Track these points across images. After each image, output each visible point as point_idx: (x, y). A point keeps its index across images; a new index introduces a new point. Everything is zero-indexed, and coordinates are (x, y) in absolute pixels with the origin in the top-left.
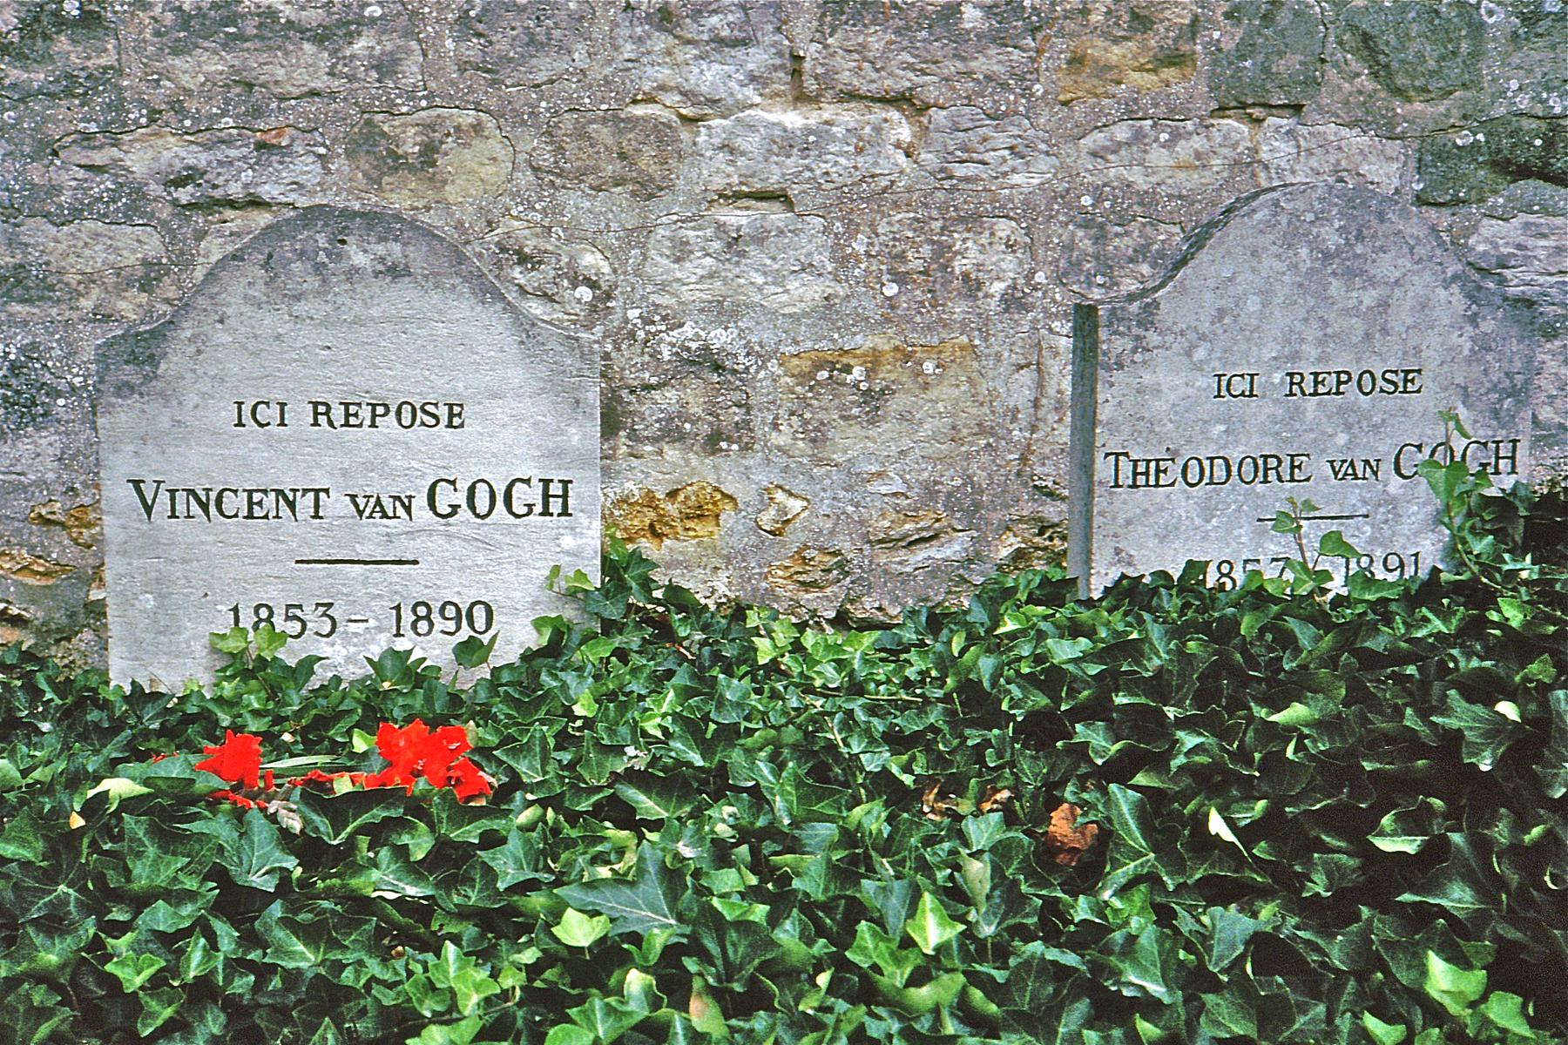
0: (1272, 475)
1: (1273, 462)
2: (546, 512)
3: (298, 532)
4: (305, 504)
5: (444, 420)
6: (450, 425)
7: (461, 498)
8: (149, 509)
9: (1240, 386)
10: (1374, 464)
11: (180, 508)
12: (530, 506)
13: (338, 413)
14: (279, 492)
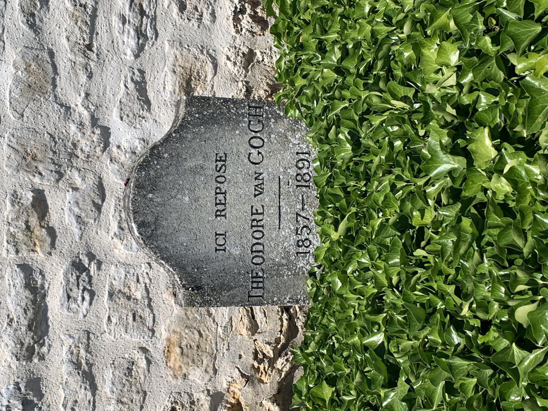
0: (259, 224)
1: (255, 223)
10: (257, 175)
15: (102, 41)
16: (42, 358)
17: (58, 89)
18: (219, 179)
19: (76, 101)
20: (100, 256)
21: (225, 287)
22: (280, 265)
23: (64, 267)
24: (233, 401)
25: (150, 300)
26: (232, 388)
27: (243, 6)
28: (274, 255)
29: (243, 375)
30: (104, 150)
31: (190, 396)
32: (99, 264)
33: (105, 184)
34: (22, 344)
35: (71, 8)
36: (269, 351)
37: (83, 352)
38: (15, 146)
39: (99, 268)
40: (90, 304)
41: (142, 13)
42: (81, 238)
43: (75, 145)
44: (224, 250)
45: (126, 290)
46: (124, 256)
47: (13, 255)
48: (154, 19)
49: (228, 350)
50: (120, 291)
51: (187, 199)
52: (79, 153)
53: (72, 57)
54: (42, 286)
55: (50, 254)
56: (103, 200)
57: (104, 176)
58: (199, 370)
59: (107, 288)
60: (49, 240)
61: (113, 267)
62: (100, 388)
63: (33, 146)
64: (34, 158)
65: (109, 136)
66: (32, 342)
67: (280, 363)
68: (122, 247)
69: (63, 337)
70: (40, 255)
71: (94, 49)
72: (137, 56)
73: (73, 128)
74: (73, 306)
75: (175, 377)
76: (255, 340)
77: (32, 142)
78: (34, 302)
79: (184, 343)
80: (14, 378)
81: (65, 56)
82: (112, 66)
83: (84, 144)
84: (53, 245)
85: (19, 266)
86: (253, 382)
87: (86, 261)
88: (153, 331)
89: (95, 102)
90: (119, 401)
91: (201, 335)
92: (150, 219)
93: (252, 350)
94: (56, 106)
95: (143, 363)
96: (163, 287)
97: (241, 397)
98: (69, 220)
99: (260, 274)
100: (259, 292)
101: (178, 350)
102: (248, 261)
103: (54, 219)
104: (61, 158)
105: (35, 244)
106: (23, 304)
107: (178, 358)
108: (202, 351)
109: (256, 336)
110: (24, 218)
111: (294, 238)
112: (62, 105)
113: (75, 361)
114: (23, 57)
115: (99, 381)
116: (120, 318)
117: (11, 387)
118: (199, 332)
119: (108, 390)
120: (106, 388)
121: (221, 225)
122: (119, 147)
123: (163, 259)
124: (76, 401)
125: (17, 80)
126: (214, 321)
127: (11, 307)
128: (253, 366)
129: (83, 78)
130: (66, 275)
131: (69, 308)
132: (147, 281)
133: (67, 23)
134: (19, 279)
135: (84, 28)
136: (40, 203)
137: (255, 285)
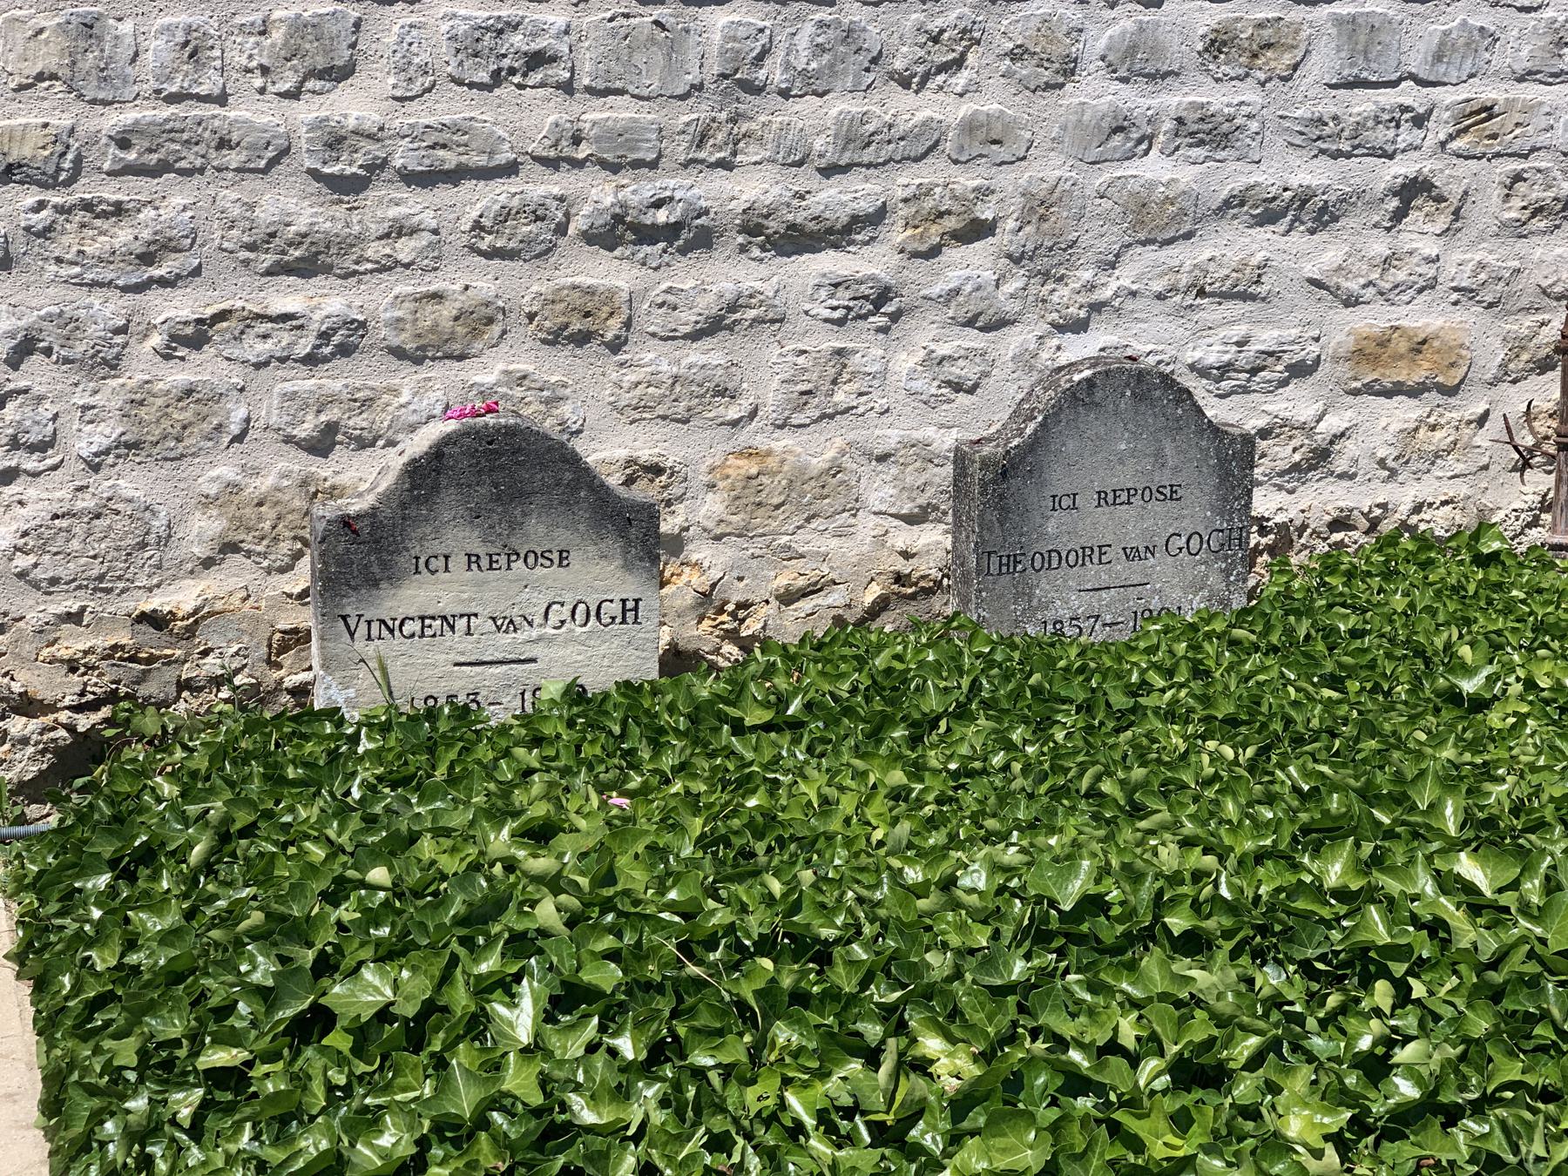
1: (1088, 552)
2: (624, 621)
3: (458, 644)
4: (461, 624)
5: (556, 561)
6: (560, 565)
7: (566, 614)
8: (352, 635)
9: (1066, 502)
11: (375, 632)
12: (613, 618)
13: (485, 562)
14: (444, 618)
15: (1211, 312)
16: (743, 249)
17: (1139, 249)
18: (1147, 492)
19: (1125, 277)
20: (896, 331)
21: (1004, 511)
22: (1031, 596)
23: (883, 275)
24: (667, 574)
25: (831, 416)
26: (687, 570)
27: (1270, 532)
28: (1043, 587)
29: (714, 586)
30: (1053, 324)
31: (680, 499)
32: (884, 330)
33: (1005, 330)
34: (767, 217)
35: (1255, 261)
36: (751, 627)
37: (752, 313)
38: (1059, 189)
39: (880, 330)
40: (826, 320)
41: (1254, 371)
42: (924, 298)
43: (1061, 279)
44: (1054, 509)
45: (846, 376)
46: (897, 369)
47: (901, 193)
48: (1245, 390)
49: (753, 557)
50: (845, 366)
51: (1123, 447)
52: (1049, 287)
53: (1187, 267)
54: (852, 243)
55: (902, 252)
56: (981, 329)
58: (722, 508)
59: (850, 345)
60: (923, 248)
61: (881, 352)
62: (694, 345)
63: (1060, 215)
64: (1043, 219)
65: (1073, 333)
66: (770, 231)
67: (730, 649)
68: (911, 364)
69: (775, 279)
70: (899, 235)
71: (1199, 301)
72: (1192, 367)
73: (1087, 275)
74: (823, 293)
75: (712, 470)
76: (767, 602)
77: (1065, 214)
78: (830, 231)
79: (764, 479)
80: (714, 206)
82: (1175, 329)
83: (1064, 292)
84: (916, 255)
85: (884, 203)
86: (701, 604)
88: (781, 427)
89: (1124, 306)
90: (676, 379)
91: (777, 507)
92: (1099, 395)
93: (751, 597)
94: (1117, 247)
95: (733, 413)
96: (851, 436)
97: (674, 588)
98: (952, 278)
99: (1019, 567)
100: (994, 569)
101: (754, 471)
102: (1037, 547)
103: (953, 254)
104: (1041, 261)
105: (916, 227)
106: (827, 214)
107: (743, 472)
108: (752, 512)
109: (774, 603)
110: (956, 208)
111: (1066, 614)
112: (1117, 256)
113: (741, 301)
114: (1184, 193)
115: (707, 343)
116: (805, 370)
117: (703, 203)
118: (782, 504)
119: (692, 359)
121: (1087, 501)
122: (1059, 348)
123: (1045, 418)
124: (675, 308)
125: (1151, 185)
126: (799, 528)
127: (822, 196)
128: (726, 602)
129: (1158, 286)
130: (872, 278)
131: (819, 286)
132: (861, 410)
133: (1233, 257)
134: (865, 206)
135: (1228, 283)
136: (977, 230)
137: (1004, 560)
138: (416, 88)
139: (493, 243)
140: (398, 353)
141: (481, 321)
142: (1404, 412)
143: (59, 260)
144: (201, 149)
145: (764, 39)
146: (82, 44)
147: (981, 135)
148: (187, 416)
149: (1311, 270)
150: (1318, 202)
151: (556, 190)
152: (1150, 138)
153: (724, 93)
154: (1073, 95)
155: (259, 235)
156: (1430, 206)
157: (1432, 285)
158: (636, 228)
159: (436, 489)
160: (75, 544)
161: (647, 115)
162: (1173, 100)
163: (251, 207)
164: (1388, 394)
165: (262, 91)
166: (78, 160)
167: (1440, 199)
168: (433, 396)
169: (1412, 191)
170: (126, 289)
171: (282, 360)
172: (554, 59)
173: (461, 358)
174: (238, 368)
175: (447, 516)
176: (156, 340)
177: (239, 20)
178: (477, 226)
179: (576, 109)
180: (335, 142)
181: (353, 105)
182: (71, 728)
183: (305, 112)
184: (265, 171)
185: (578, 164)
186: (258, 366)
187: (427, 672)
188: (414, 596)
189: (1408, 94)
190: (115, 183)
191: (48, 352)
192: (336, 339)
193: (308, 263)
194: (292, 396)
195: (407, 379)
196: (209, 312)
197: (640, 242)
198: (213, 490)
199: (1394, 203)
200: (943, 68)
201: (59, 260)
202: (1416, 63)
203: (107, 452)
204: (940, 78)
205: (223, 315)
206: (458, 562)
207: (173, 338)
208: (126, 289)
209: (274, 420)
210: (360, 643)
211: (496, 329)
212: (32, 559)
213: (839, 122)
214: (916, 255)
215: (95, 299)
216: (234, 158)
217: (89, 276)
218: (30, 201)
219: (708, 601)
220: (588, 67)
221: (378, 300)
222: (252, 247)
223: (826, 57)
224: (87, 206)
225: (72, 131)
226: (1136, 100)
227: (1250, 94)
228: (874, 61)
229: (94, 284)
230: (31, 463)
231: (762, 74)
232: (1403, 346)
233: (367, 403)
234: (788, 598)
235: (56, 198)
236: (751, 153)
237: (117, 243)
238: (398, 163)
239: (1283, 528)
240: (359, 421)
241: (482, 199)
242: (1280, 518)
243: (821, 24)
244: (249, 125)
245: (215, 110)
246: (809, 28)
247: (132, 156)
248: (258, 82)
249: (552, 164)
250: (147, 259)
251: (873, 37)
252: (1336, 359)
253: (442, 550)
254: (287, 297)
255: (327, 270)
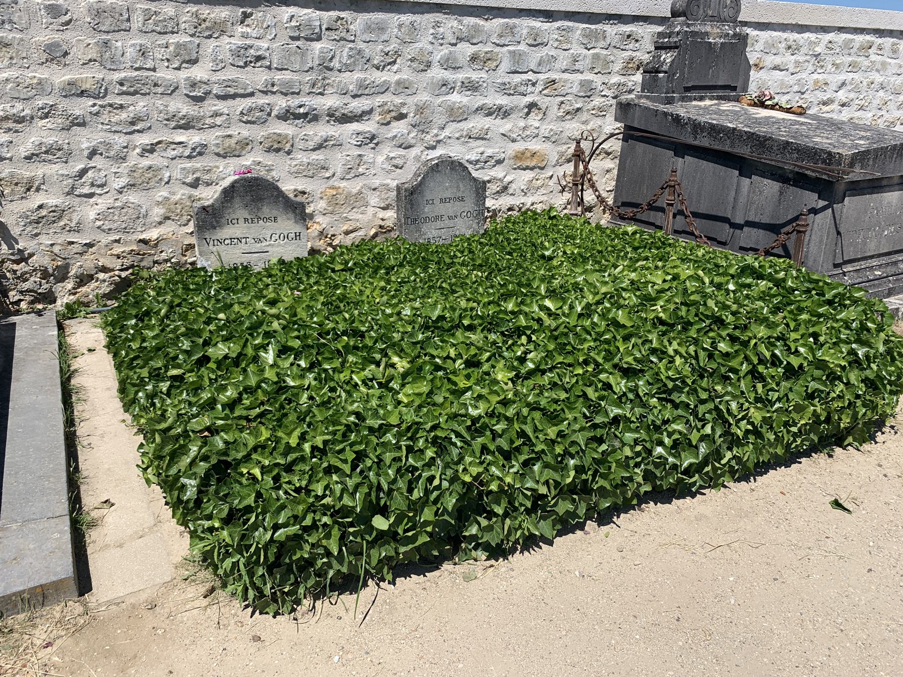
3: (243, 247)
7: (277, 236)
13: (250, 221)
15: (473, 143)
16: (328, 122)
19: (447, 132)
31: (312, 202)
32: (374, 148)
37: (332, 143)
41: (486, 162)
47: (377, 104)
48: (483, 168)
57: (414, 148)
64: (422, 113)
70: (378, 118)
73: (435, 131)
75: (321, 193)
78: (355, 116)
81: (466, 126)
83: (428, 137)
84: (383, 124)
87: (375, 141)
90: (309, 163)
95: (327, 175)
96: (365, 182)
103: (395, 124)
104: (421, 126)
115: (317, 152)
120: (315, 156)
121: (437, 201)
125: (454, 103)
127: (352, 105)
129: (457, 135)
130: (369, 131)
133: (479, 126)
134: (366, 108)
136: (401, 117)
138: (219, 67)
139: (248, 119)
140: (218, 155)
141: (245, 144)
142: (529, 175)
143: (102, 123)
144: (148, 86)
145: (332, 53)
146: (104, 49)
147: (402, 86)
148: (150, 175)
149: (502, 131)
150: (504, 109)
151: (267, 102)
152: (454, 88)
153: (320, 70)
154: (430, 73)
155: (170, 116)
156: (537, 111)
157: (537, 136)
158: (293, 114)
159: (232, 197)
160: (116, 218)
161: (296, 77)
162: (460, 76)
163: (167, 106)
164: (524, 169)
165: (168, 67)
166: (106, 89)
167: (540, 109)
168: (230, 169)
169: (532, 106)
170: (126, 133)
171: (180, 157)
172: (264, 58)
173: (239, 156)
174: (166, 160)
175: (237, 206)
176: (138, 150)
177: (158, 43)
178: (242, 113)
179: (273, 75)
180: (193, 85)
181: (199, 72)
182: (119, 276)
183: (183, 75)
184: (170, 94)
185: (274, 93)
186: (172, 159)
187: (234, 256)
188: (227, 232)
189: (530, 76)
190: (119, 98)
191: (101, 154)
192: (197, 150)
193: (187, 125)
194: (184, 169)
195: (221, 163)
196: (155, 141)
197: (295, 119)
198: (160, 200)
199: (526, 110)
200: (389, 64)
201: (102, 123)
202: (533, 66)
203: (124, 187)
204: (389, 67)
205: (159, 142)
206: (241, 221)
207: (143, 150)
208: (126, 133)
209: (178, 177)
210: (211, 247)
211: (250, 147)
212: (102, 222)
213: (357, 81)
214: (383, 124)
215: (116, 136)
216: (160, 90)
217: (113, 129)
218: (91, 103)
219: (322, 234)
220: (276, 61)
221: (211, 137)
222: (168, 120)
223: (353, 59)
224: (111, 105)
225: (103, 80)
226: (449, 75)
227: (484, 75)
228: (368, 61)
229: (115, 132)
230: (99, 191)
231: (332, 64)
232: (529, 155)
233: (209, 171)
234: (347, 233)
235: (99, 102)
236: (329, 90)
237: (122, 118)
238: (215, 92)
239: (494, 210)
240: (206, 177)
241: (243, 104)
242: (493, 208)
243: (350, 48)
244: (165, 79)
245: (152, 73)
246: (347, 50)
247: (125, 88)
248: (166, 64)
249: (265, 93)
250: (133, 123)
251: (367, 53)
252: (509, 159)
253: (236, 217)
254: (180, 136)
255: (193, 127)
